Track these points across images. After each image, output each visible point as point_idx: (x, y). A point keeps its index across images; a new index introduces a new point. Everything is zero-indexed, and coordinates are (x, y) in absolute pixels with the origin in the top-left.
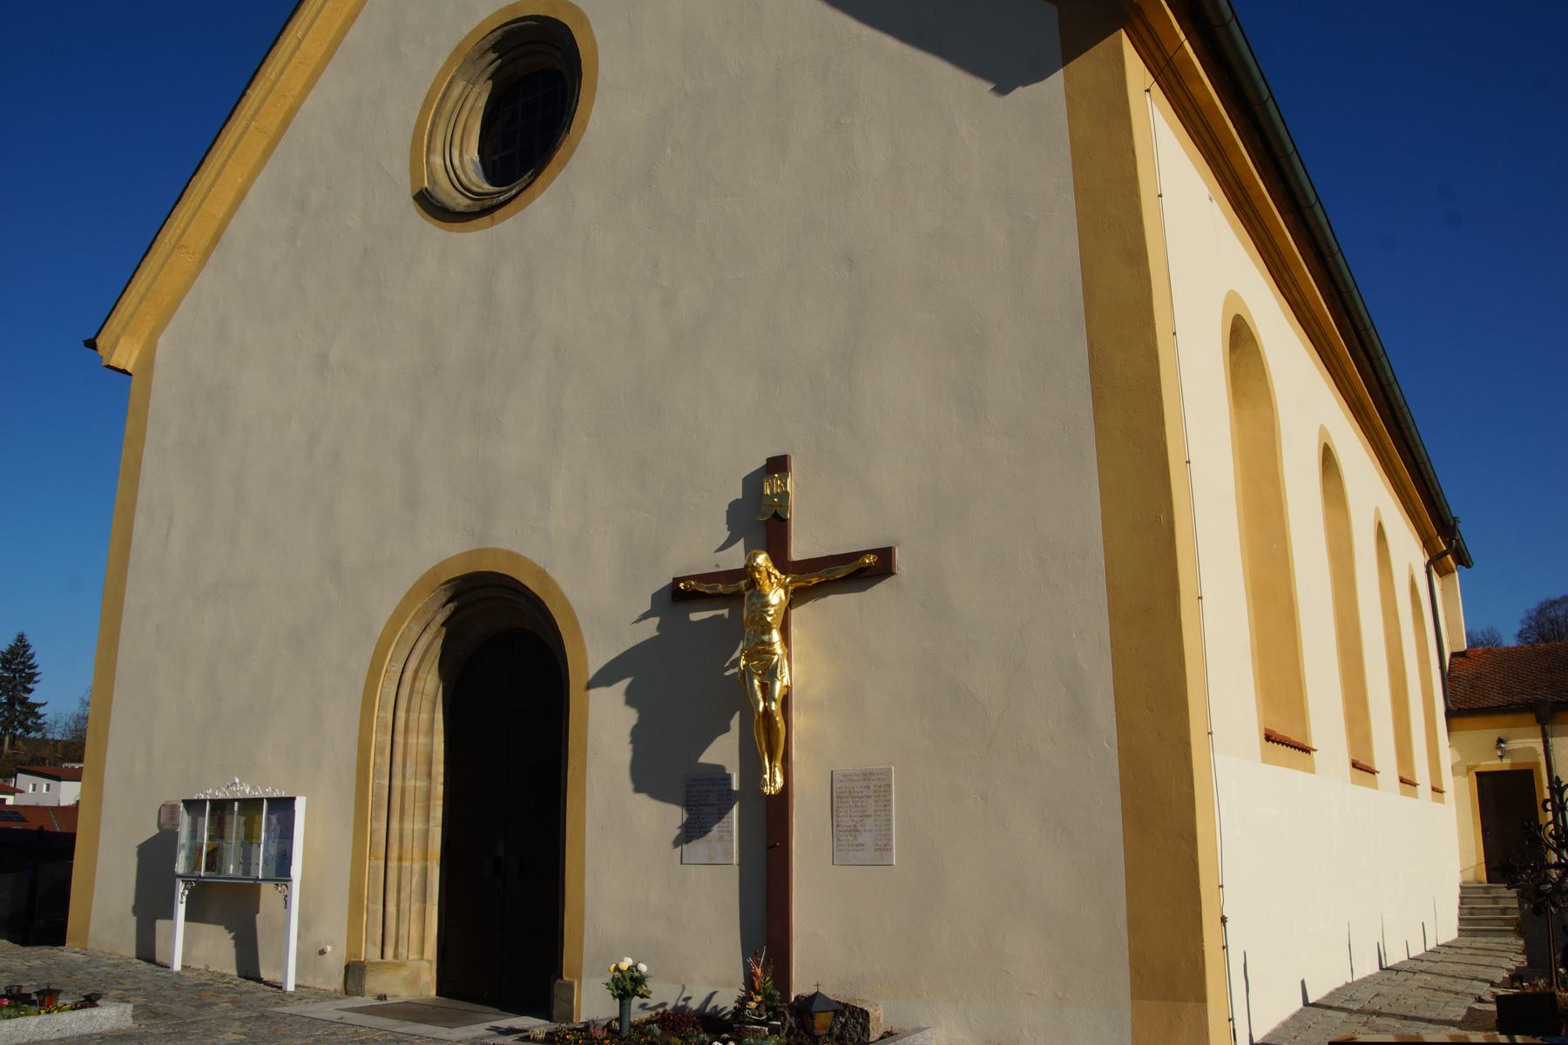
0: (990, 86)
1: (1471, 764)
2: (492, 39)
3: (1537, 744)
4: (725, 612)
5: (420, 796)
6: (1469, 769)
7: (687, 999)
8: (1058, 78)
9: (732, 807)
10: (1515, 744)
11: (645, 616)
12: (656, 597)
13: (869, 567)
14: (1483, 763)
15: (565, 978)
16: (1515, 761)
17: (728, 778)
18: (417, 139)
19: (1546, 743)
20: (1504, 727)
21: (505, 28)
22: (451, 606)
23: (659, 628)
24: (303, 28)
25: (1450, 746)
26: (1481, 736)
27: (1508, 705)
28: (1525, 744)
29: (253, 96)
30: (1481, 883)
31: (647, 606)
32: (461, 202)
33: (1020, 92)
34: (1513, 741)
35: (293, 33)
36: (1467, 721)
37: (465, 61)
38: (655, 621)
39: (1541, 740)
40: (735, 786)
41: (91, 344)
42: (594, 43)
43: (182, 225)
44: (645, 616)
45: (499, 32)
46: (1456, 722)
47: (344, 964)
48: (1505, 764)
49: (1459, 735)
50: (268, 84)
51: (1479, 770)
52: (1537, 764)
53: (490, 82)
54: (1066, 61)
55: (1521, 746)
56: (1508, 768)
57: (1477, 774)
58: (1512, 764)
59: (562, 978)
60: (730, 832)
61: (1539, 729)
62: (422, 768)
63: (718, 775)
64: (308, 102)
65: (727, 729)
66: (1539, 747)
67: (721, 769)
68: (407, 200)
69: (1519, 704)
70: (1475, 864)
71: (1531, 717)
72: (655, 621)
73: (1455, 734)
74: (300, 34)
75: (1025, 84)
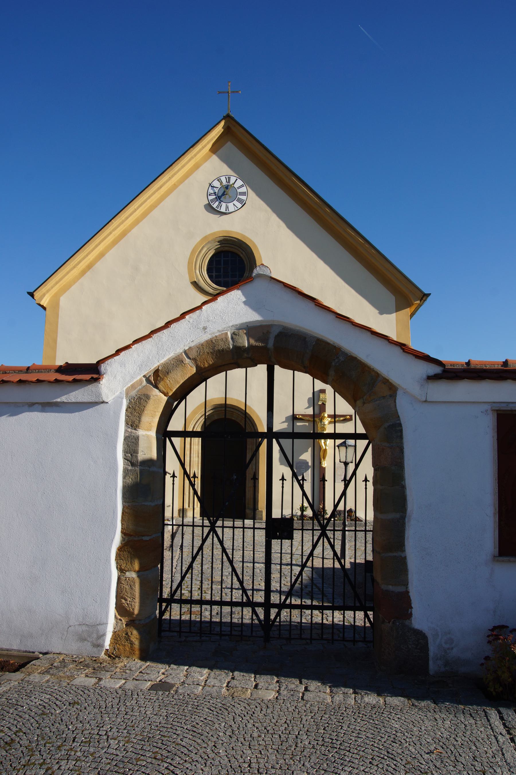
0: (378, 312)
2: (219, 239)
4: (307, 424)
5: (196, 462)
7: (297, 513)
8: (394, 315)
9: (309, 469)
11: (283, 422)
12: (287, 418)
13: (348, 419)
15: (260, 509)
17: (308, 463)
21: (225, 238)
22: (212, 411)
23: (287, 426)
24: (137, 205)
29: (115, 223)
31: (284, 420)
33: (385, 315)
35: (134, 206)
38: (287, 424)
40: (310, 464)
41: (32, 295)
42: (261, 256)
43: (78, 260)
44: (283, 422)
45: (222, 238)
47: (178, 509)
50: (121, 221)
53: (214, 251)
54: (396, 311)
59: (258, 509)
60: (308, 475)
62: (197, 455)
63: (305, 463)
64: (134, 231)
65: (307, 451)
67: (306, 460)
72: (286, 424)
74: (136, 207)
75: (386, 314)
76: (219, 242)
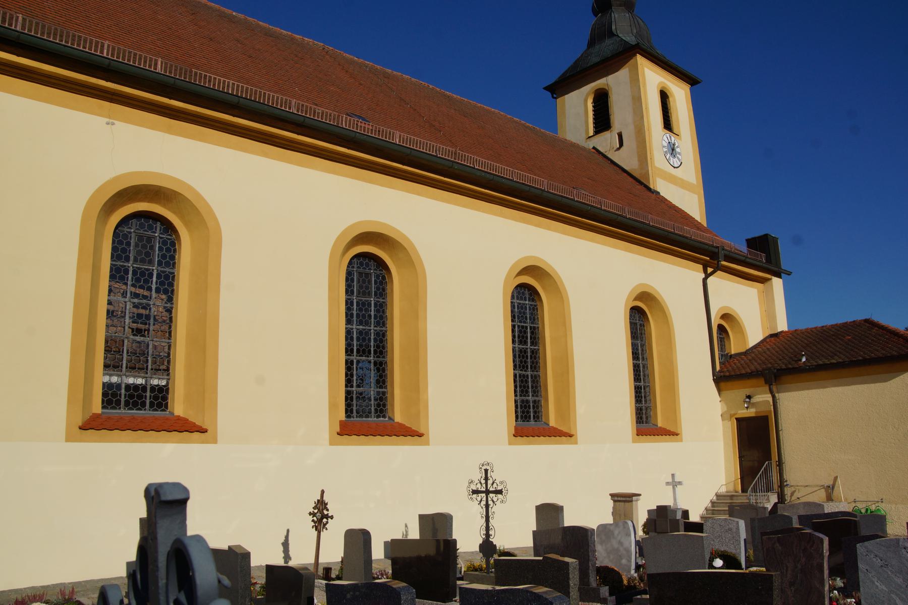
1: (733, 412)
3: (768, 397)
6: (731, 416)
10: (757, 399)
14: (739, 412)
16: (758, 411)
19: (774, 397)
20: (752, 387)
25: (720, 401)
26: (738, 393)
27: (752, 372)
28: (763, 397)
30: (737, 492)
34: (756, 397)
36: (729, 384)
39: (770, 395)
46: (722, 385)
48: (751, 412)
49: (726, 393)
51: (737, 416)
52: (770, 412)
55: (761, 400)
56: (753, 415)
57: (736, 419)
58: (756, 412)
61: (767, 388)
66: (770, 400)
69: (758, 371)
70: (734, 479)
71: (762, 381)
73: (724, 393)
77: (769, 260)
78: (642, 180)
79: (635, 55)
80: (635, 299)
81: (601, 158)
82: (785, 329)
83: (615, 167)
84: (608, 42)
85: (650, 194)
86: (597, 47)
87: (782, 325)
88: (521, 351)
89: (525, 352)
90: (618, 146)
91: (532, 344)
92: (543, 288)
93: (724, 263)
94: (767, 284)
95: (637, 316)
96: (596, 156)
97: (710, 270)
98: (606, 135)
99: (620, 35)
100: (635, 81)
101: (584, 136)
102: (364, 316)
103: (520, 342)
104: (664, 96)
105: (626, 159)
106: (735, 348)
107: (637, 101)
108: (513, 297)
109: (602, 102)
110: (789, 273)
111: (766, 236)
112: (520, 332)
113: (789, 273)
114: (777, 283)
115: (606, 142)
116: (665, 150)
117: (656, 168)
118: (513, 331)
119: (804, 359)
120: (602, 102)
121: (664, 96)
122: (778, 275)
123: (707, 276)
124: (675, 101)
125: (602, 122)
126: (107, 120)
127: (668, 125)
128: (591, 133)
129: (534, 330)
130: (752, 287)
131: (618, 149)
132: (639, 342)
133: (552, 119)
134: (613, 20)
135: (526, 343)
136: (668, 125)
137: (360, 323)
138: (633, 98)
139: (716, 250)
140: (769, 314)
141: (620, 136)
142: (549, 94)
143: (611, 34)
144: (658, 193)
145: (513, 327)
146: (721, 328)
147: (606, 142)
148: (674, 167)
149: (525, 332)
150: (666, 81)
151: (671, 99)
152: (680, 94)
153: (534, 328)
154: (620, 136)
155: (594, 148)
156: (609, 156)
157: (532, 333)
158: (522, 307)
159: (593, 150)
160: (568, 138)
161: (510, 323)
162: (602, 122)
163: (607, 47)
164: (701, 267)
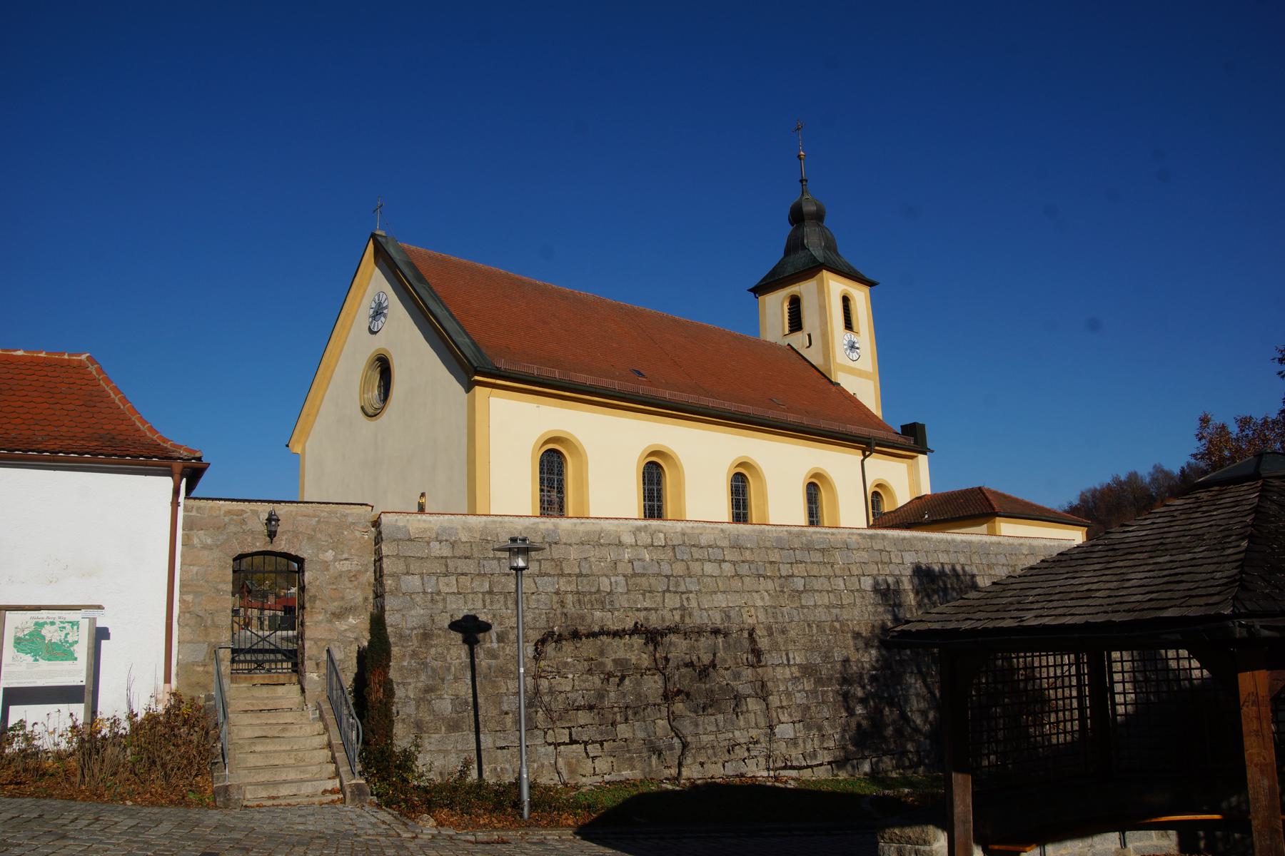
18: (360, 389)
32: (371, 411)
37: (371, 365)
41: (287, 446)
68: (360, 409)
76: (377, 360)
77: (916, 442)
78: (825, 374)
79: (821, 270)
80: (811, 477)
81: (795, 355)
82: (929, 492)
83: (806, 363)
84: (801, 254)
85: (831, 386)
86: (792, 256)
87: (926, 489)
88: (737, 513)
89: (740, 514)
90: (808, 345)
91: (744, 509)
92: (750, 475)
93: (877, 448)
94: (915, 459)
95: (812, 488)
96: (791, 352)
97: (867, 453)
98: (798, 335)
99: (811, 249)
100: (822, 292)
101: (781, 334)
102: (651, 497)
103: (736, 509)
104: (846, 300)
105: (813, 356)
106: (887, 507)
107: (823, 309)
108: (732, 481)
109: (795, 303)
110: (932, 451)
111: (914, 423)
112: (736, 502)
113: (932, 451)
114: (923, 460)
115: (798, 340)
116: (846, 347)
117: (837, 363)
118: (732, 502)
119: (926, 516)
120: (795, 303)
121: (846, 300)
122: (925, 453)
123: (865, 457)
124: (855, 304)
125: (796, 323)
126: (536, 405)
127: (849, 325)
128: (787, 332)
129: (744, 501)
130: (903, 462)
131: (808, 347)
132: (814, 506)
133: (754, 318)
134: (805, 234)
135: (740, 509)
136: (849, 325)
137: (649, 501)
138: (820, 306)
139: (870, 441)
140: (914, 481)
141: (809, 336)
142: (752, 294)
143: (804, 247)
144: (839, 384)
145: (732, 499)
146: (876, 494)
147: (798, 340)
148: (853, 361)
149: (739, 502)
150: (845, 287)
151: (852, 302)
152: (861, 297)
153: (745, 499)
154: (809, 336)
155: (789, 345)
156: (800, 352)
157: (744, 502)
158: (737, 487)
159: (788, 347)
160: (768, 340)
161: (730, 497)
162: (796, 323)
163: (799, 259)
164: (860, 452)
